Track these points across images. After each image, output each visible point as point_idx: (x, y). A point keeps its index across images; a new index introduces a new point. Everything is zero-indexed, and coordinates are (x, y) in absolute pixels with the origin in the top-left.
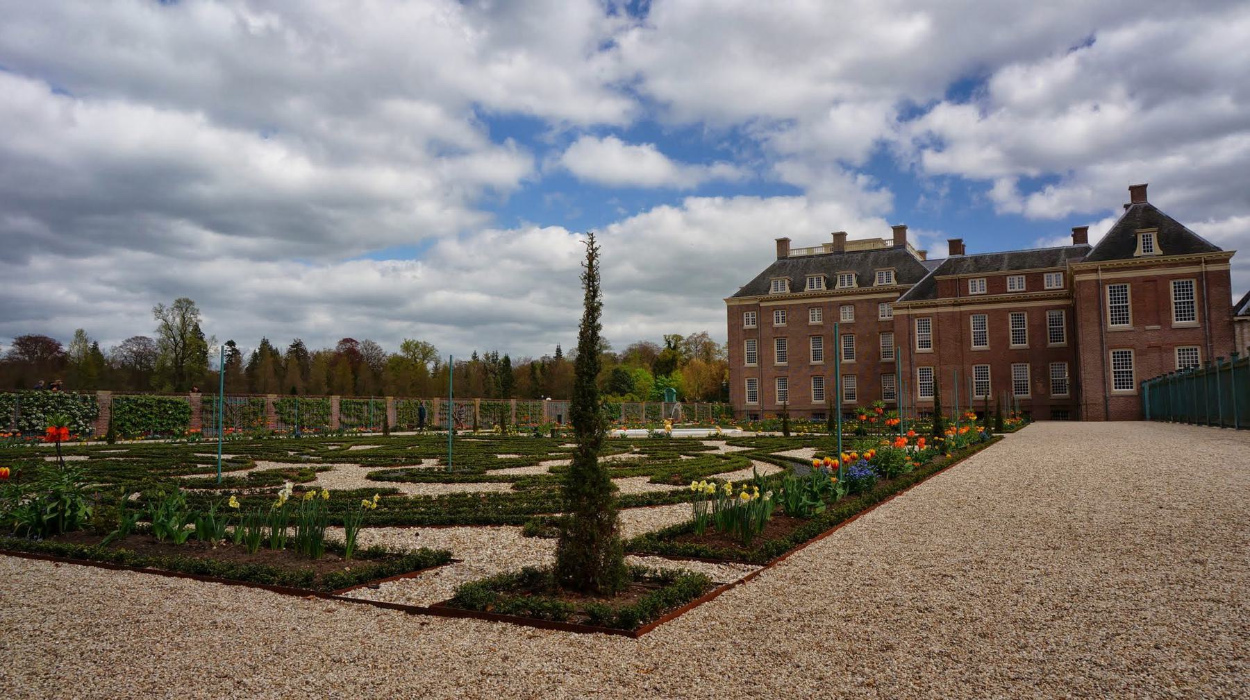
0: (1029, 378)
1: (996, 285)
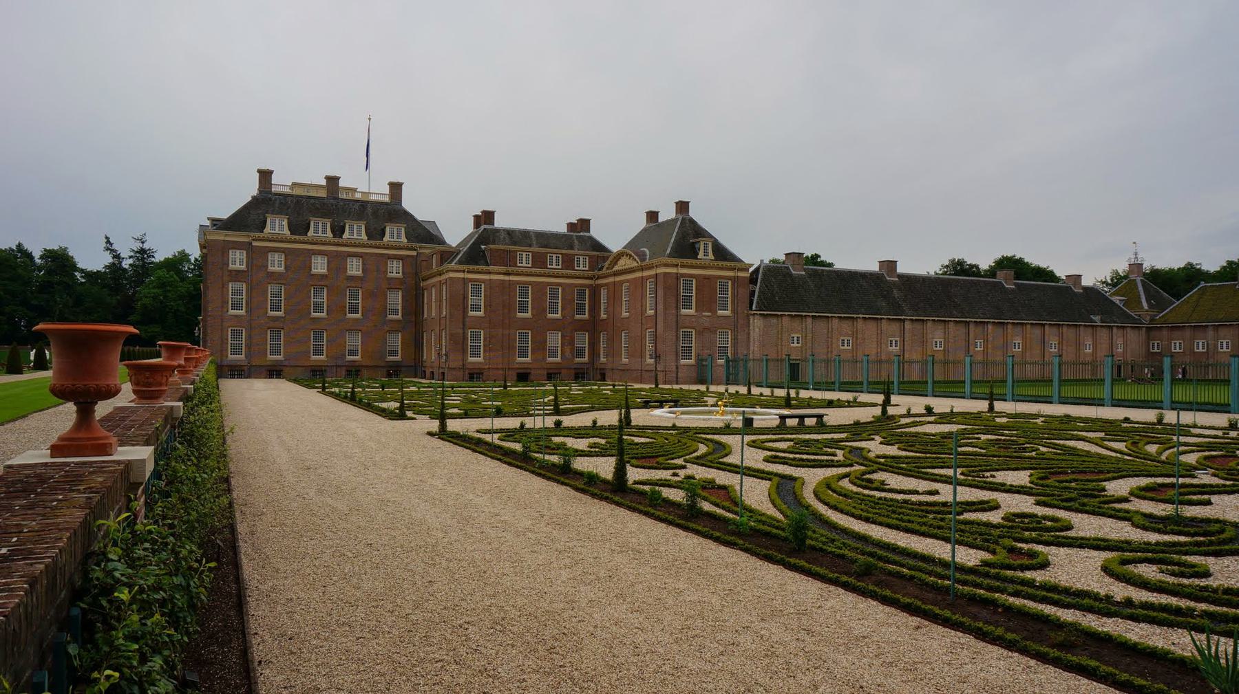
0: (560, 345)
1: (539, 261)
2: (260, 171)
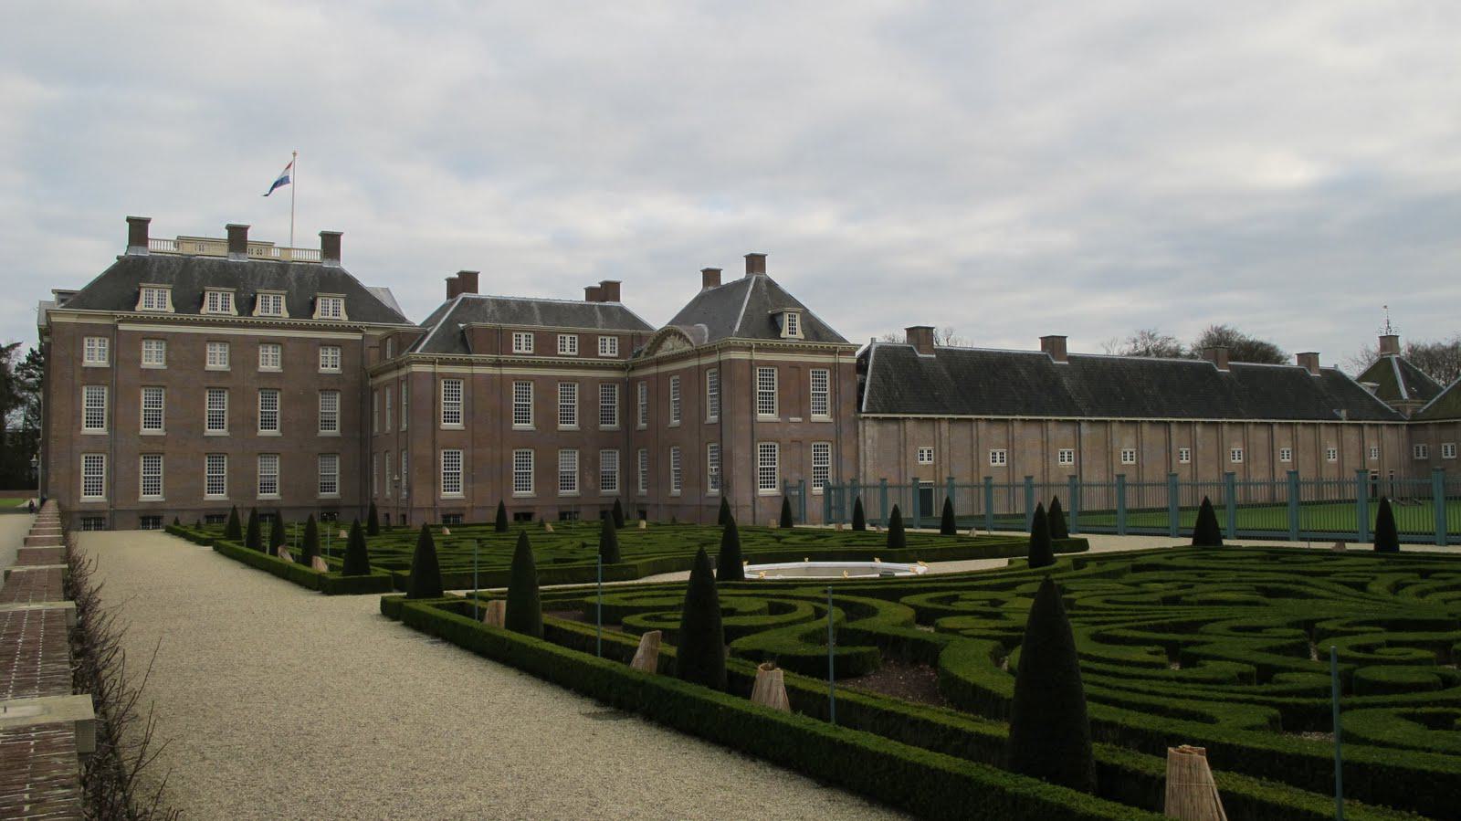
0: (577, 469)
1: (545, 343)
2: (129, 220)
